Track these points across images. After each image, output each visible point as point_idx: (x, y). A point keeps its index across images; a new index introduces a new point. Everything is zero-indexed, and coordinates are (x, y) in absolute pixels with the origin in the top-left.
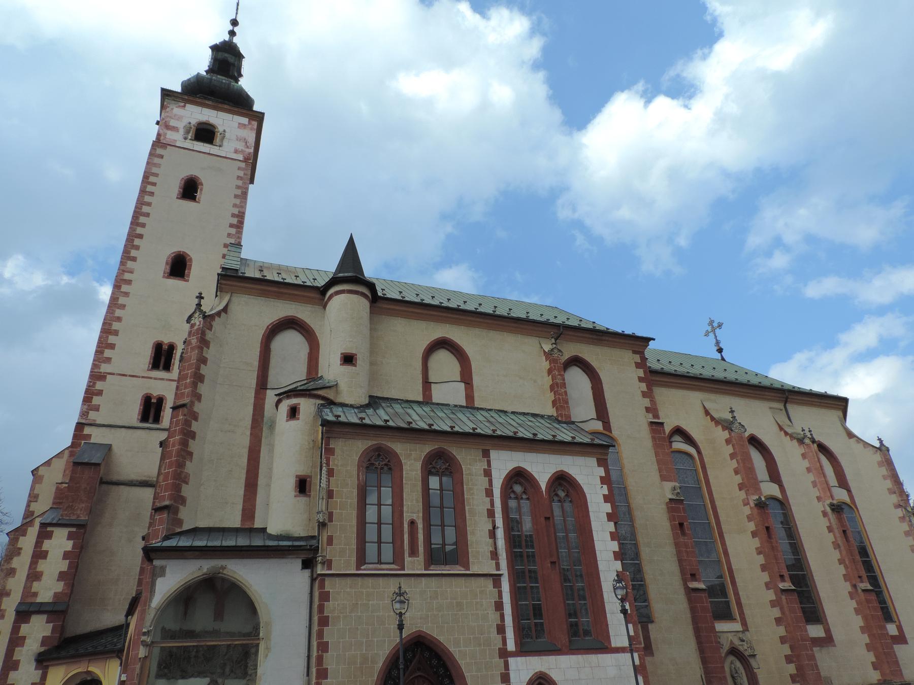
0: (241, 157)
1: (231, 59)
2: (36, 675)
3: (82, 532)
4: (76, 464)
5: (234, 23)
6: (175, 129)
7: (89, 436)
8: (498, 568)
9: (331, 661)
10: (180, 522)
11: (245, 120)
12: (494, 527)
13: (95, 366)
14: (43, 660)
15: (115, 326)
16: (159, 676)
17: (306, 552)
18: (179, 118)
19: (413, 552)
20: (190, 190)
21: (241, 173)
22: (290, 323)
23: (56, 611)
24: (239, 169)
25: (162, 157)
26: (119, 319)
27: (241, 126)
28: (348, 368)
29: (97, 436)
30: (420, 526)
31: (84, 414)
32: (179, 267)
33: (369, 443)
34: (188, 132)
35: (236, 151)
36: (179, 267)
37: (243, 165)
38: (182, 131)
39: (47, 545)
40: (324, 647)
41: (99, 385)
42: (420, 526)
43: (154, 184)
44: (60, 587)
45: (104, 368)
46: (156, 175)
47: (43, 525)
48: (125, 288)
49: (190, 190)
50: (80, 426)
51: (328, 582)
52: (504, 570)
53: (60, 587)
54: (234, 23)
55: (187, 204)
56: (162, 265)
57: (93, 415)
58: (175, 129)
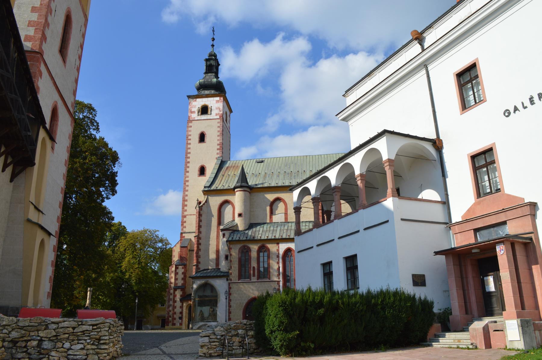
0: (218, 117)
1: (213, 62)
2: (180, 304)
3: (185, 266)
4: (181, 247)
5: (213, 39)
6: (194, 112)
7: (184, 237)
8: (279, 279)
9: (232, 303)
10: (199, 268)
11: (218, 98)
12: (279, 267)
13: (183, 213)
14: (182, 300)
15: (186, 198)
16: (198, 306)
17: (226, 276)
18: (195, 107)
19: (254, 275)
20: (202, 138)
21: (219, 125)
22: (226, 202)
23: (183, 288)
24: (218, 123)
25: (191, 127)
26: (187, 195)
27: (217, 101)
28: (240, 218)
29: (187, 236)
30: (256, 268)
31: (182, 229)
32: (202, 171)
33: (242, 245)
34: (198, 112)
35: (216, 115)
36: (202, 171)
37: (219, 120)
38: (197, 112)
39: (178, 271)
40: (230, 300)
41: (185, 219)
42: (256, 268)
43: (190, 139)
44: (182, 282)
45: (186, 213)
46: (190, 135)
47: (176, 266)
48: (187, 184)
49: (202, 138)
50: (182, 233)
51: (231, 284)
52: (281, 279)
53: (182, 282)
54: (213, 39)
55: (202, 144)
56: (197, 172)
57: (184, 229)
58: (194, 112)
